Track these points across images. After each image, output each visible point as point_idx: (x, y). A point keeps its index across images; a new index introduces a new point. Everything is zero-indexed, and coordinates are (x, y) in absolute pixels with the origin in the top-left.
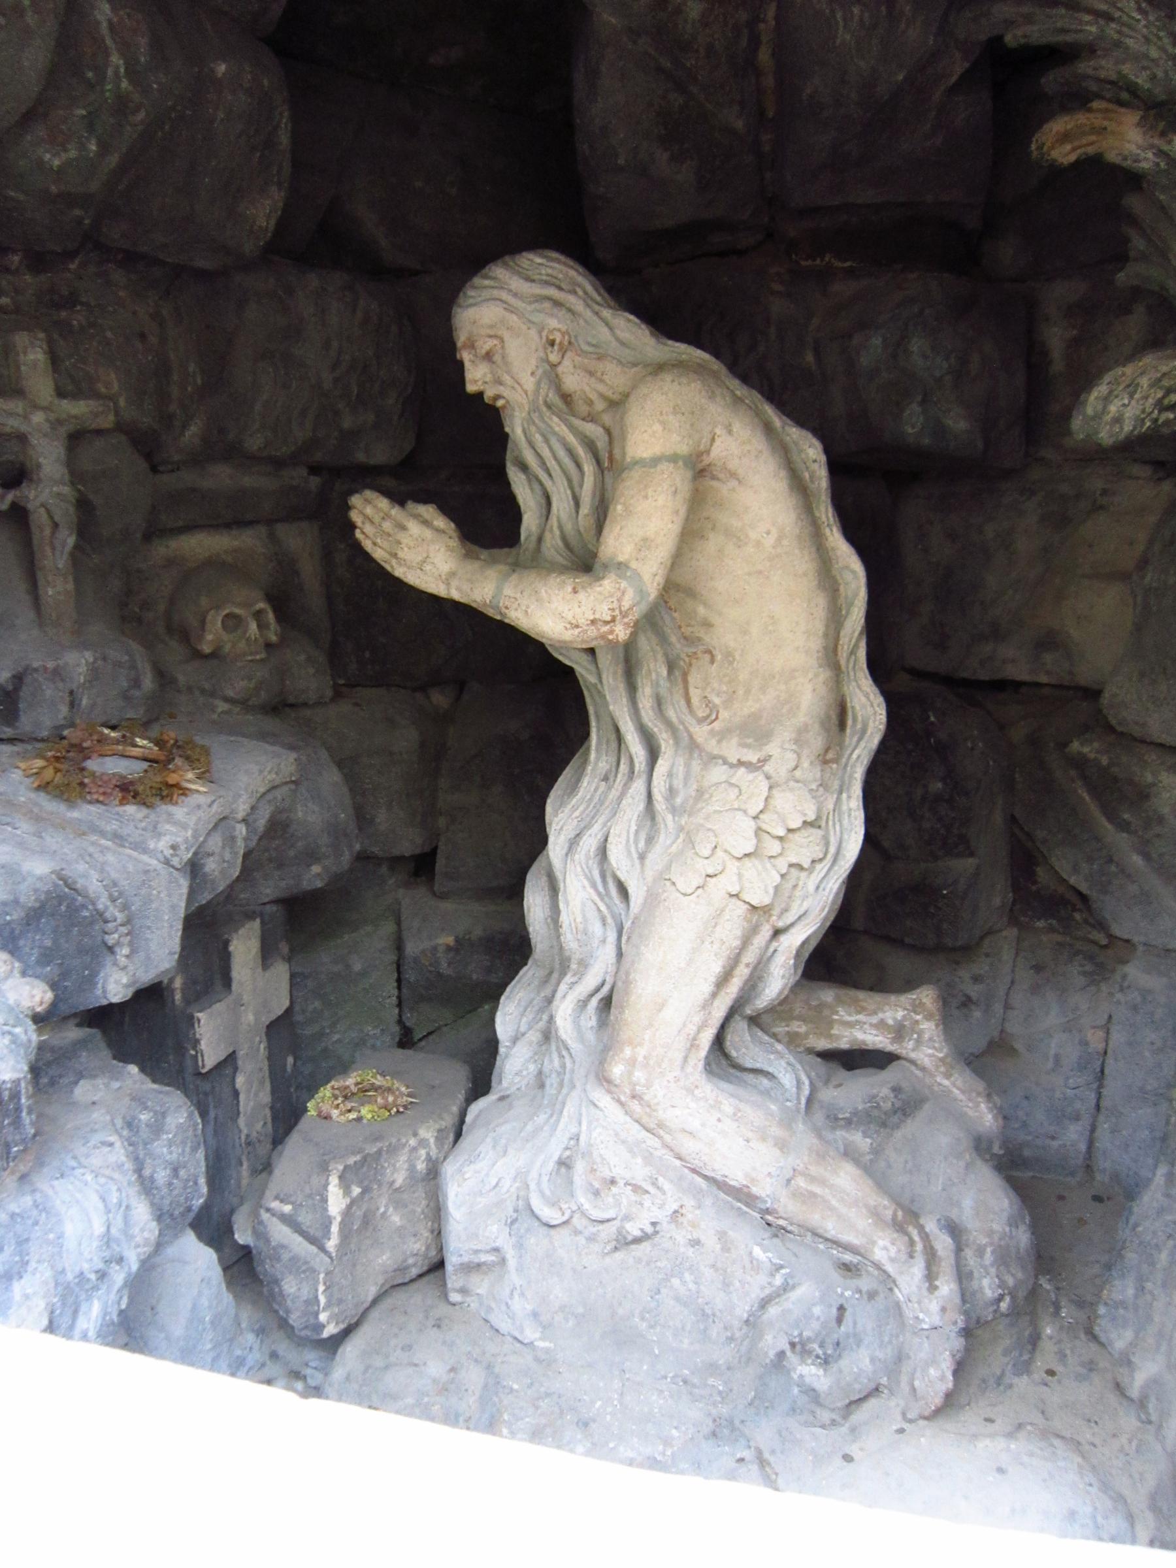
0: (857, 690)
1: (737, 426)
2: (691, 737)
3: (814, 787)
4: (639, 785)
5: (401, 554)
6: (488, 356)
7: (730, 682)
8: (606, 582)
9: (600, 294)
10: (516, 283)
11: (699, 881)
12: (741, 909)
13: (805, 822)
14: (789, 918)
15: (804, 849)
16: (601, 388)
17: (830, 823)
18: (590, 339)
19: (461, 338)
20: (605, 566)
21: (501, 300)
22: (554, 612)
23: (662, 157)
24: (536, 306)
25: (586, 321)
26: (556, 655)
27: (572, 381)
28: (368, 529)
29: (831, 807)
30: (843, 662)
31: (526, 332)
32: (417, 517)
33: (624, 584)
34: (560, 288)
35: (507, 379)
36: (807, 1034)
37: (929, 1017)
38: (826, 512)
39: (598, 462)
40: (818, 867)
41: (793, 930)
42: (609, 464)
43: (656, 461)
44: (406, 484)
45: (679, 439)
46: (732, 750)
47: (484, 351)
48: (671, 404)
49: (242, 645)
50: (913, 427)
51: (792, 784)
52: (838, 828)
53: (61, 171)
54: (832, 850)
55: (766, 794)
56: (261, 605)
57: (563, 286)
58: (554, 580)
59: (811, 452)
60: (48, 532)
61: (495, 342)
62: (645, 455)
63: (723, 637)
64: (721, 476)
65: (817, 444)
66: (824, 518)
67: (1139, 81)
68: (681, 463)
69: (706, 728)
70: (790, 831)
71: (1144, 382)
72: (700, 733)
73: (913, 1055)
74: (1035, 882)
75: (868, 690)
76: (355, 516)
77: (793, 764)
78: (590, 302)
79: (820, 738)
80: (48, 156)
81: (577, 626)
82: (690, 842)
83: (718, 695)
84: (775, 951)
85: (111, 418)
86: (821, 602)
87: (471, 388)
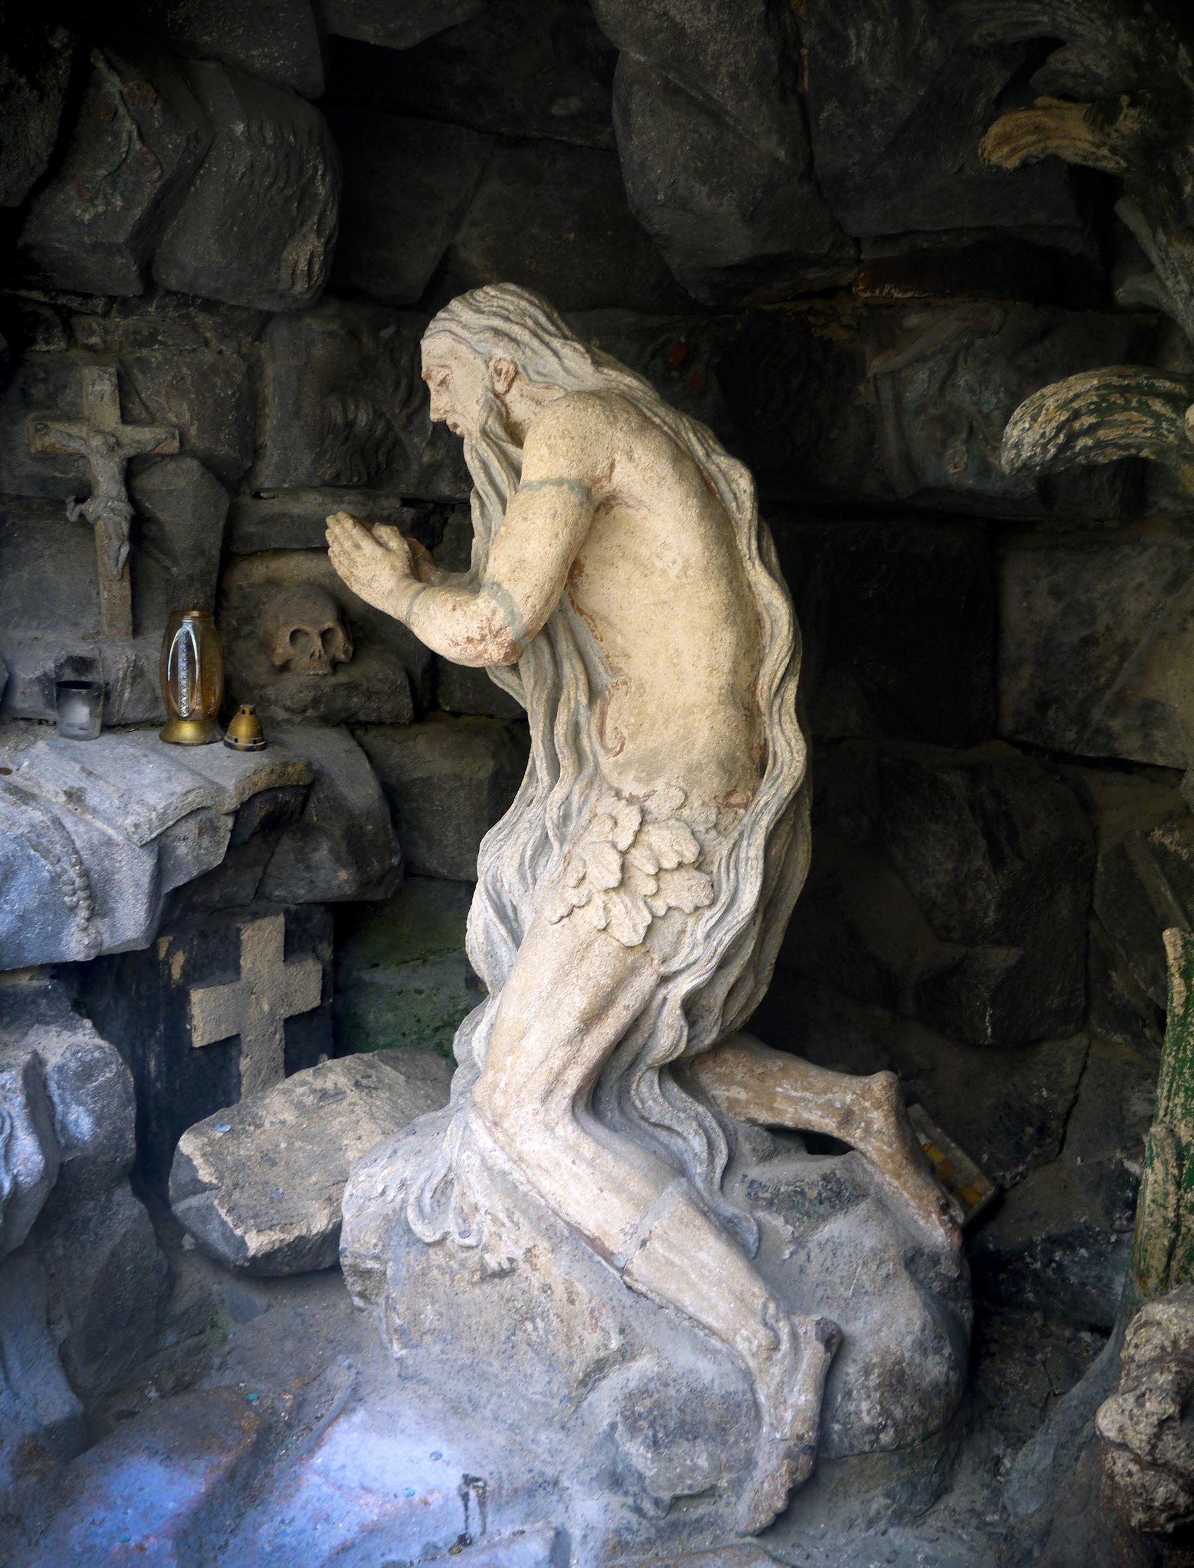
0: (780, 735)
1: (639, 452)
2: (597, 765)
3: (702, 829)
5: (356, 572)
7: (638, 714)
8: (480, 601)
9: (553, 323)
11: (563, 911)
13: (680, 865)
14: (675, 965)
15: (684, 891)
17: (723, 869)
18: (541, 369)
21: (450, 332)
23: (701, 190)
24: (481, 336)
25: (533, 351)
26: (491, 677)
27: (520, 409)
29: (725, 852)
30: (763, 704)
33: (493, 603)
34: (507, 319)
35: (459, 408)
36: (748, 1102)
37: (877, 1105)
38: (746, 543)
40: (708, 914)
41: (680, 979)
43: (542, 483)
45: (566, 463)
47: (438, 381)
48: (561, 428)
50: (955, 467)
51: (672, 821)
52: (732, 875)
54: (724, 898)
55: (636, 828)
57: (512, 317)
59: (739, 483)
61: (448, 372)
62: (533, 479)
63: (638, 667)
64: (632, 503)
66: (745, 551)
67: (1099, 71)
68: (565, 487)
69: (612, 759)
71: (1050, 403)
73: (861, 1146)
74: (1111, 990)
75: (791, 735)
76: (329, 537)
77: (678, 802)
78: (539, 332)
79: (716, 780)
80: (79, 212)
81: (457, 644)
83: (626, 727)
84: (665, 999)
85: (176, 444)
86: (727, 640)
87: (434, 417)
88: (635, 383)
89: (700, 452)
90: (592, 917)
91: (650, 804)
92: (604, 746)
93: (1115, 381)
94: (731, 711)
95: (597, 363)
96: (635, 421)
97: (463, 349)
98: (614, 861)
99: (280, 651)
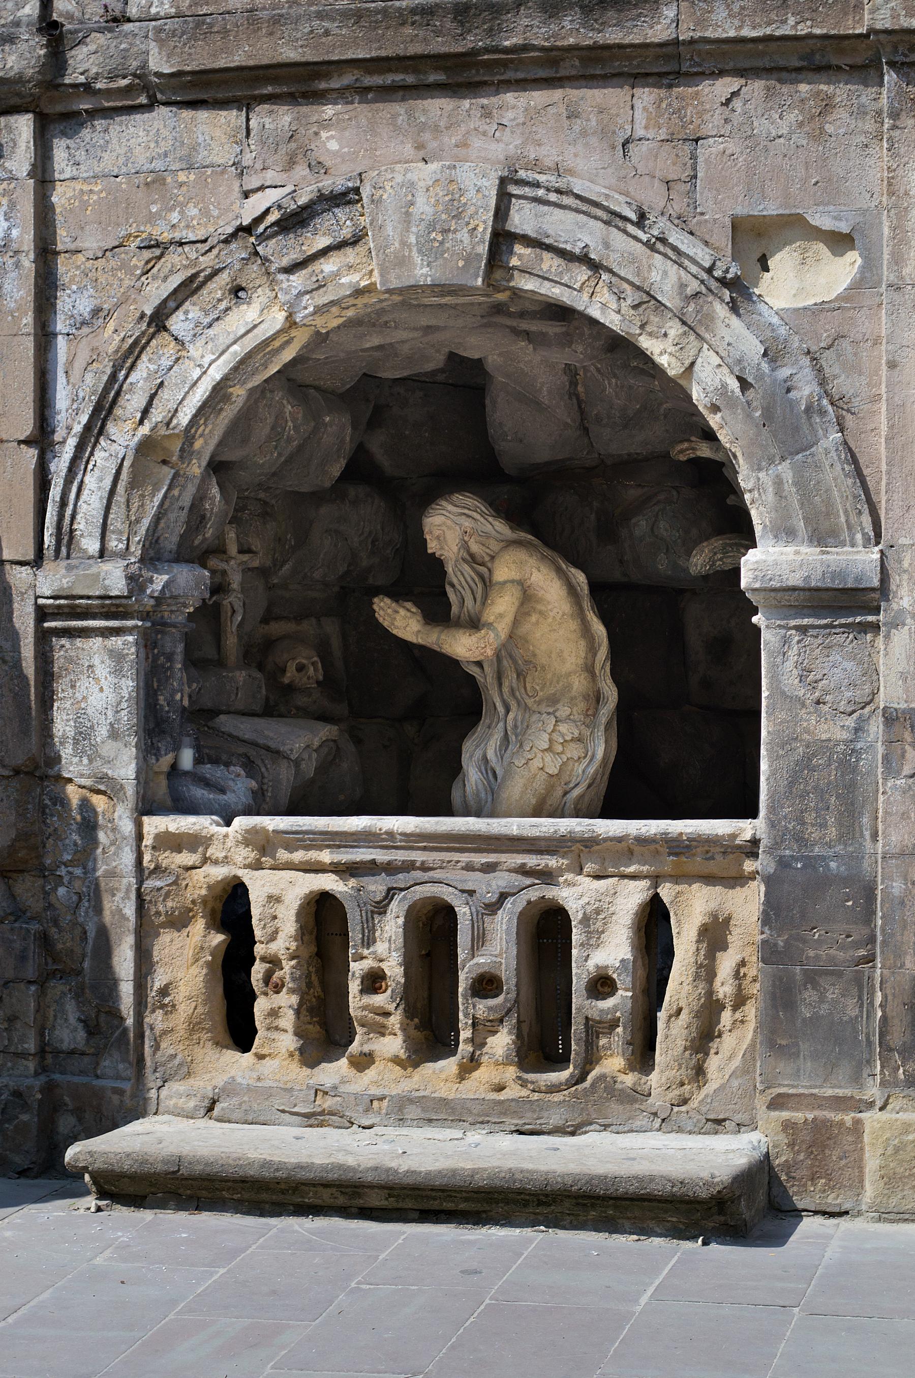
1: (542, 568)
4: (501, 724)
6: (438, 538)
10: (450, 507)
11: (523, 761)
12: (542, 776)
15: (574, 751)
16: (487, 551)
19: (426, 530)
20: (484, 625)
22: (463, 646)
27: (475, 548)
28: (381, 613)
30: (597, 672)
31: (453, 527)
32: (404, 607)
33: (490, 632)
34: (469, 509)
35: (446, 548)
38: (587, 604)
39: (485, 584)
42: (487, 583)
43: (505, 582)
44: (397, 594)
46: (543, 708)
49: (305, 679)
53: (263, 464)
56: (315, 659)
58: (461, 631)
59: (580, 578)
60: (229, 614)
65: (583, 575)
70: (566, 741)
72: (530, 702)
76: (375, 607)
82: (521, 746)
87: (429, 551)
88: (533, 538)
89: (564, 566)
90: (536, 763)
91: (558, 714)
92: (528, 695)
93: (728, 541)
94: (586, 674)
95: (511, 528)
96: (539, 555)
97: (449, 522)
98: (546, 737)
99: (288, 675)
